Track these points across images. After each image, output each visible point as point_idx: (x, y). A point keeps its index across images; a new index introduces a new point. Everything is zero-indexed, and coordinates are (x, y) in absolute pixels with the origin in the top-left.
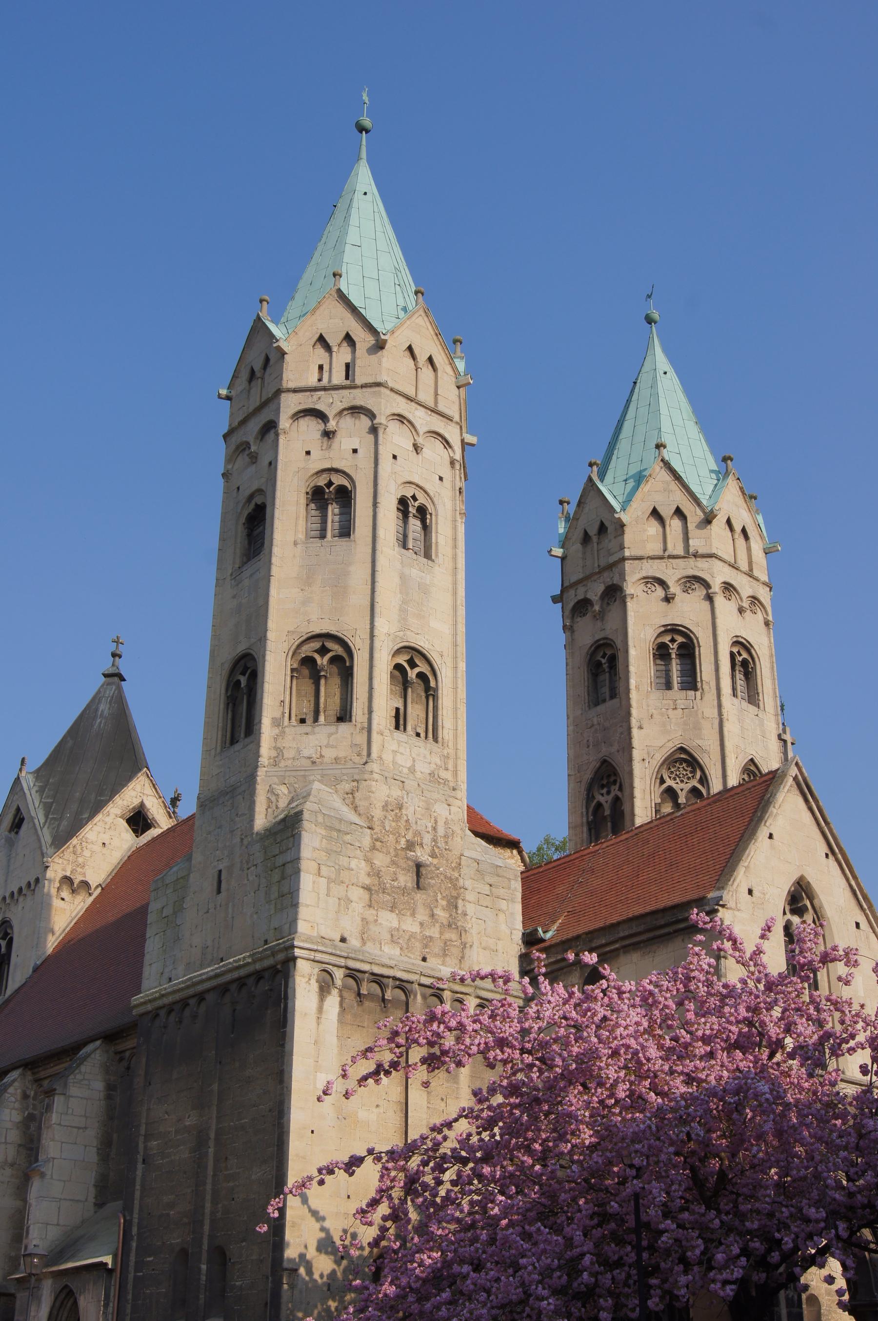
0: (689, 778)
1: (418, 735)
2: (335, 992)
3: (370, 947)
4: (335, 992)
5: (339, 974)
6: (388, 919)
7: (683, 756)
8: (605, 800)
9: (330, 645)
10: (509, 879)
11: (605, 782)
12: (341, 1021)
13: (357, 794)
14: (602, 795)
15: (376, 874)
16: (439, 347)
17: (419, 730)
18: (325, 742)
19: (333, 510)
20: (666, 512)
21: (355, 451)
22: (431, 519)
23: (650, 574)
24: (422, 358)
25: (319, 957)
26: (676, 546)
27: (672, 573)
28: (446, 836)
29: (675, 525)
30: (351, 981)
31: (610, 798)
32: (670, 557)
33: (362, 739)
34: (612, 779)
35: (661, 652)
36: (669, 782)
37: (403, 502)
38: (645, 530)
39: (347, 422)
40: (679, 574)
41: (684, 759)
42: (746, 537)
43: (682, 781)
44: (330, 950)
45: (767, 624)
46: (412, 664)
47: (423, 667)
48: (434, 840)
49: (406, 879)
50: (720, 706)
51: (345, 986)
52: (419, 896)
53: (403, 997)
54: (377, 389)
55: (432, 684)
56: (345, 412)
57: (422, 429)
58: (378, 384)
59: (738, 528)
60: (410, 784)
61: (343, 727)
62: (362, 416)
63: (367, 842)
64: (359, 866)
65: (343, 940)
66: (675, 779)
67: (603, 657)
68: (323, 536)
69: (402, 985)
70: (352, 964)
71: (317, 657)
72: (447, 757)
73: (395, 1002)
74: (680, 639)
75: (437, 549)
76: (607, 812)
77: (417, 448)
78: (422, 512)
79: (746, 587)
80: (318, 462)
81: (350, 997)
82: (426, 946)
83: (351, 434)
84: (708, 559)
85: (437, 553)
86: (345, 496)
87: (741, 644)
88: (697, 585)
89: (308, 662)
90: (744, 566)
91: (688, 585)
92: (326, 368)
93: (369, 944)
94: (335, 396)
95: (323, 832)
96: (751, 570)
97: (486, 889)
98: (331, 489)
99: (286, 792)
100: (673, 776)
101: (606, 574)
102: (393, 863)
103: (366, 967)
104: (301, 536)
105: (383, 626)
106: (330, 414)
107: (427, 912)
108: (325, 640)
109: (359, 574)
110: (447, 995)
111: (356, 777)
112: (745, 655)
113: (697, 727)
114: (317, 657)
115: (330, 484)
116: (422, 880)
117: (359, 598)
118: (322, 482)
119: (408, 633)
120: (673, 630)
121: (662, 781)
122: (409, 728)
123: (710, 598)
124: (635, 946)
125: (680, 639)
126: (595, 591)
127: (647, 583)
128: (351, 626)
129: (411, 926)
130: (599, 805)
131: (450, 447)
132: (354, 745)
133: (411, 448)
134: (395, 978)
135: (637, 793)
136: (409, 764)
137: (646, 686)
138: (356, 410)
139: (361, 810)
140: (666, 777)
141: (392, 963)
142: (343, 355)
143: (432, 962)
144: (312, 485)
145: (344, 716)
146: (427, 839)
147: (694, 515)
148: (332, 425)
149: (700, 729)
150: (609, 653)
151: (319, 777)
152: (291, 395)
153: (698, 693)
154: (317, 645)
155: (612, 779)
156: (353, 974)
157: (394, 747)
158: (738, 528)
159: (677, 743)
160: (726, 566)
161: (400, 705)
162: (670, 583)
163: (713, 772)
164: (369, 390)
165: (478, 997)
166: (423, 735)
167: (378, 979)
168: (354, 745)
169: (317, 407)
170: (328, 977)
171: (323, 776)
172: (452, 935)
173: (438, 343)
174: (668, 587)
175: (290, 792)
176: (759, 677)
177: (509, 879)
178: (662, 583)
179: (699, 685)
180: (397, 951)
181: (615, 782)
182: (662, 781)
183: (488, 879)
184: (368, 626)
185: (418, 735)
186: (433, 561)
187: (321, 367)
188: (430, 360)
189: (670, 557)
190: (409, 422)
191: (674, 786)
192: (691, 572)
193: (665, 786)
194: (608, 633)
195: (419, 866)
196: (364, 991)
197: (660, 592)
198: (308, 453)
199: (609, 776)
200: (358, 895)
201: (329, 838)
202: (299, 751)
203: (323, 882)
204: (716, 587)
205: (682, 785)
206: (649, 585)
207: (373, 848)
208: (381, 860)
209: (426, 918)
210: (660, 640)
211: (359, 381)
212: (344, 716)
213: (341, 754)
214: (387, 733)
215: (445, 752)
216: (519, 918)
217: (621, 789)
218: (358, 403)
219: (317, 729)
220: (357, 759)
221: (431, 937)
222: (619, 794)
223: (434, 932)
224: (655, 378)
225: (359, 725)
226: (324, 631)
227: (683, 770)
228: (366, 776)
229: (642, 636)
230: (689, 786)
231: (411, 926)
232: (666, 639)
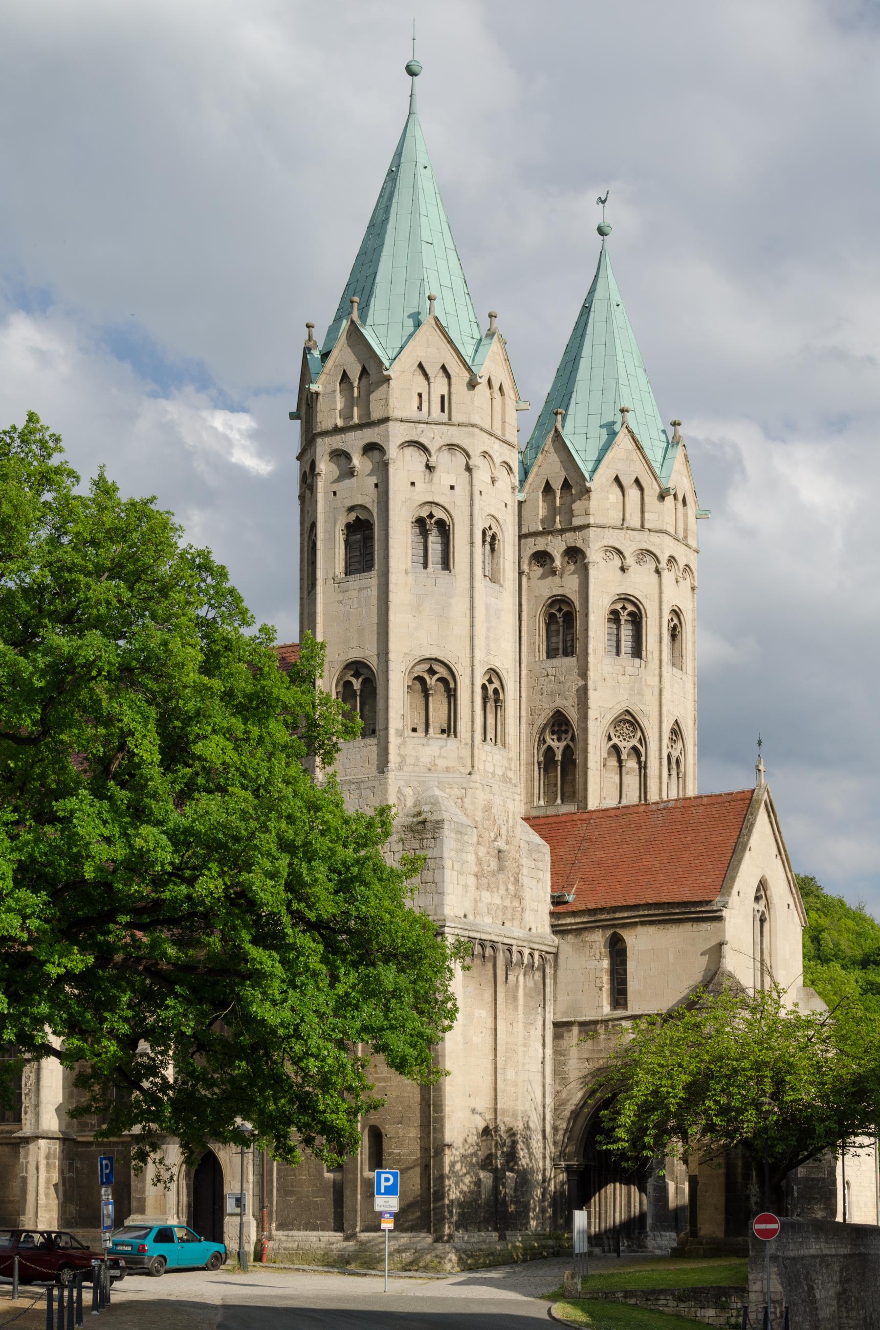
0: (630, 737)
3: (478, 920)
6: (486, 896)
7: (627, 718)
8: (559, 747)
9: (437, 667)
10: (544, 854)
11: (556, 729)
13: (465, 800)
14: (553, 740)
15: (479, 863)
16: (507, 372)
18: (437, 754)
19: (434, 539)
20: (627, 481)
21: (452, 488)
22: (499, 544)
23: (611, 544)
24: (496, 387)
25: (457, 931)
26: (634, 520)
27: (630, 544)
28: (513, 827)
29: (633, 493)
31: (562, 745)
32: (628, 528)
33: (466, 753)
34: (563, 728)
35: (615, 617)
36: (615, 740)
37: (484, 533)
38: (608, 499)
39: (445, 456)
40: (635, 546)
41: (629, 721)
42: (684, 503)
43: (624, 739)
44: (463, 927)
45: (693, 589)
46: (490, 681)
47: (496, 684)
48: (508, 831)
49: (494, 865)
50: (661, 676)
52: (501, 877)
53: (492, 953)
54: (471, 429)
55: (501, 697)
56: (444, 448)
57: (498, 461)
58: (473, 425)
59: (680, 498)
60: (495, 787)
61: (452, 742)
62: (458, 453)
63: (475, 839)
64: (471, 858)
65: (465, 916)
66: (619, 737)
68: (425, 566)
71: (426, 677)
72: (510, 759)
74: (630, 608)
75: (504, 575)
76: (559, 757)
77: (493, 481)
78: (494, 537)
79: (683, 556)
80: (422, 493)
83: (449, 469)
84: (660, 534)
85: (504, 577)
86: (444, 529)
87: (676, 613)
88: (648, 558)
89: (420, 679)
90: (681, 535)
91: (641, 557)
92: (425, 397)
93: (478, 917)
94: (436, 431)
95: (453, 835)
96: (686, 537)
97: (532, 864)
98: (433, 521)
99: (411, 793)
100: (618, 734)
103: (477, 935)
104: (410, 564)
105: (479, 655)
106: (433, 449)
107: (505, 888)
108: (432, 664)
109: (460, 606)
110: (514, 949)
111: (465, 785)
112: (676, 621)
113: (641, 693)
114: (426, 677)
115: (431, 516)
117: (461, 628)
118: (424, 514)
119: (491, 657)
120: (625, 599)
121: (610, 739)
123: (658, 572)
125: (630, 608)
127: (607, 551)
128: (455, 654)
129: (497, 901)
130: (550, 750)
131: (512, 473)
132: (460, 758)
133: (490, 481)
134: (491, 941)
135: (591, 749)
136: (491, 770)
137: (601, 652)
138: (452, 447)
139: (469, 813)
140: (612, 735)
141: (489, 930)
142: (440, 386)
144: (416, 515)
145: (449, 730)
146: (504, 831)
147: (652, 490)
148: (433, 461)
149: (642, 695)
151: (436, 783)
152: (399, 424)
153: (643, 662)
154: (427, 667)
155: (563, 728)
157: (484, 758)
158: (680, 498)
159: (624, 706)
160: (671, 539)
163: (650, 735)
164: (464, 429)
166: (493, 740)
168: (460, 758)
169: (421, 440)
171: (439, 782)
172: (516, 903)
173: (505, 368)
174: (624, 557)
175: (414, 794)
176: (684, 641)
177: (544, 854)
178: (619, 552)
179: (644, 653)
180: (490, 921)
181: (566, 732)
182: (610, 739)
183: (535, 856)
184: (468, 655)
186: (502, 586)
187: (420, 395)
188: (501, 389)
189: (628, 528)
190: (490, 456)
191: (619, 744)
192: (645, 546)
193: (611, 743)
195: (499, 852)
197: (617, 562)
198: (413, 484)
199: (560, 725)
200: (471, 881)
201: (457, 840)
202: (417, 759)
203: (455, 873)
204: (664, 559)
205: (625, 743)
206: (608, 553)
207: (479, 843)
208: (482, 851)
210: (614, 607)
211: (456, 419)
212: (449, 730)
213: (451, 764)
215: (510, 755)
216: (549, 883)
217: (573, 739)
218: (456, 442)
219: (431, 742)
220: (462, 769)
221: (506, 907)
222: (571, 744)
223: (507, 903)
224: (609, 311)
225: (463, 741)
226: (433, 656)
227: (626, 729)
228: (472, 785)
229: (600, 603)
230: (631, 744)
232: (618, 607)
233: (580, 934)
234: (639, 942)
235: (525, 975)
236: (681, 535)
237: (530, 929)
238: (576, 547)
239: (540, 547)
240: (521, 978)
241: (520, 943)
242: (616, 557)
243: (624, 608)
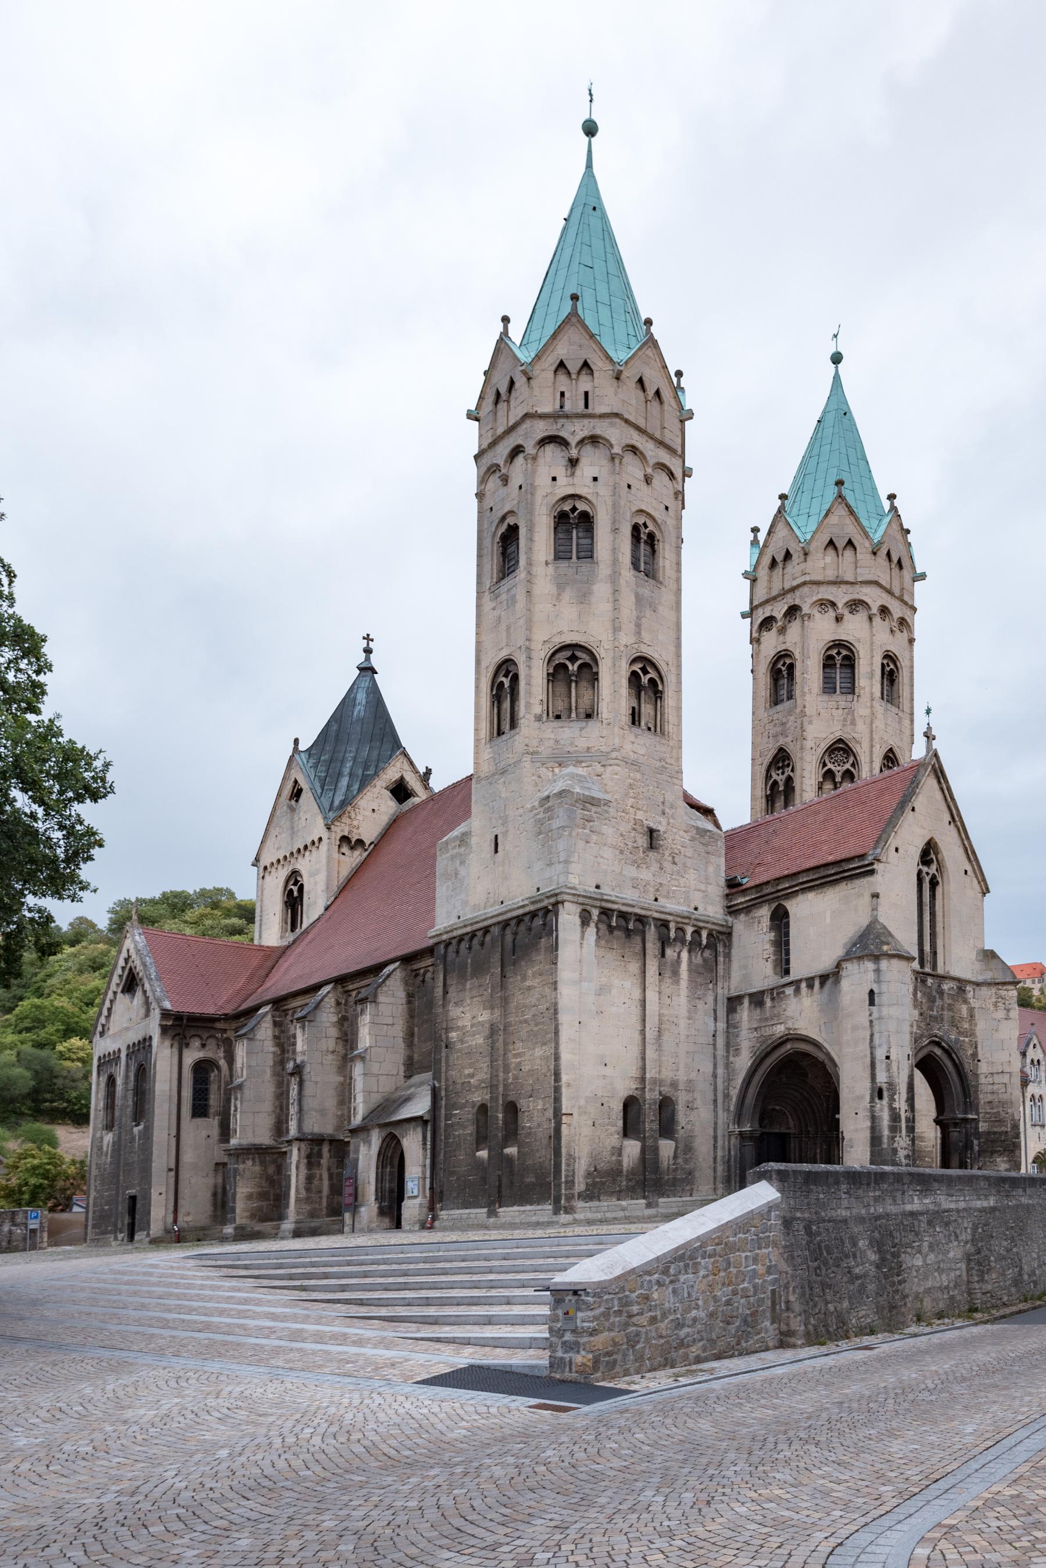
1: (649, 729)
2: (592, 925)
4: (592, 925)
5: (595, 913)
6: (631, 871)
12: (597, 946)
17: (650, 725)
25: (581, 900)
27: (841, 596)
30: (604, 917)
49: (643, 841)
51: (599, 921)
55: (660, 688)
65: (598, 887)
69: (641, 919)
70: (604, 904)
73: (634, 931)
81: (603, 927)
82: (657, 890)
101: (789, 596)
102: (634, 829)
103: (615, 907)
110: (672, 925)
116: (654, 842)
122: (643, 724)
124: (810, 889)
126: (779, 610)
134: (636, 914)
141: (634, 903)
143: (662, 901)
156: (605, 912)
161: (636, 705)
162: (840, 605)
165: (694, 926)
167: (623, 916)
170: (587, 914)
178: (833, 604)
185: (649, 729)
194: (789, 646)
195: (651, 832)
196: (614, 924)
209: (658, 869)
214: (626, 727)
225: (605, 722)
231: (645, 875)
233: (750, 911)
234: (804, 909)
235: (690, 951)
236: (897, 591)
237: (696, 909)
238: (795, 605)
239: (768, 614)
240: (685, 955)
241: (679, 920)
242: (831, 610)
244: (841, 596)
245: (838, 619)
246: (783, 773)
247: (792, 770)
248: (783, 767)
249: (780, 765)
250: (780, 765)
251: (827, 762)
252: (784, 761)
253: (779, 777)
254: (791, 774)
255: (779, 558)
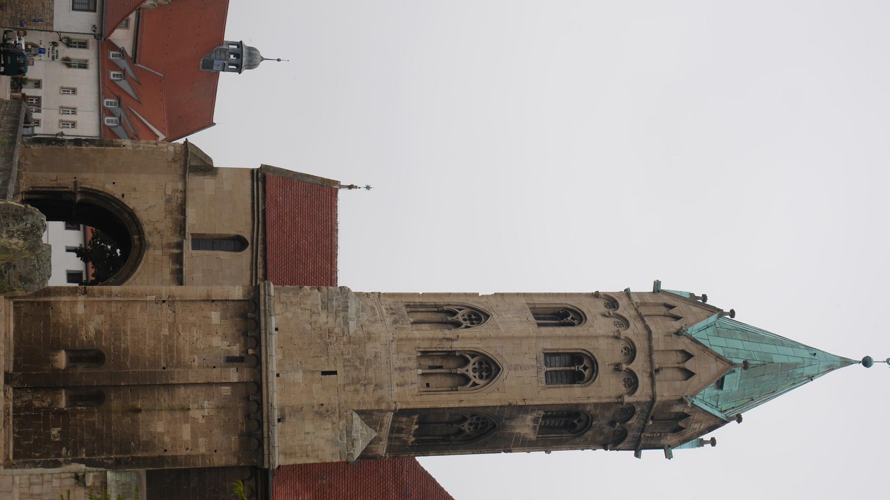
27: (639, 365)
35: (576, 358)
67: (572, 318)
74: (587, 373)
150: (576, 322)
178: (631, 360)
232: (586, 362)
243: (585, 368)
244: (639, 365)
245: (617, 368)
246: (465, 320)
247: (467, 327)
248: (470, 319)
249: (473, 317)
250: (473, 317)
251: (476, 359)
252: (476, 319)
253: (459, 317)
254: (464, 326)
255: (672, 311)
